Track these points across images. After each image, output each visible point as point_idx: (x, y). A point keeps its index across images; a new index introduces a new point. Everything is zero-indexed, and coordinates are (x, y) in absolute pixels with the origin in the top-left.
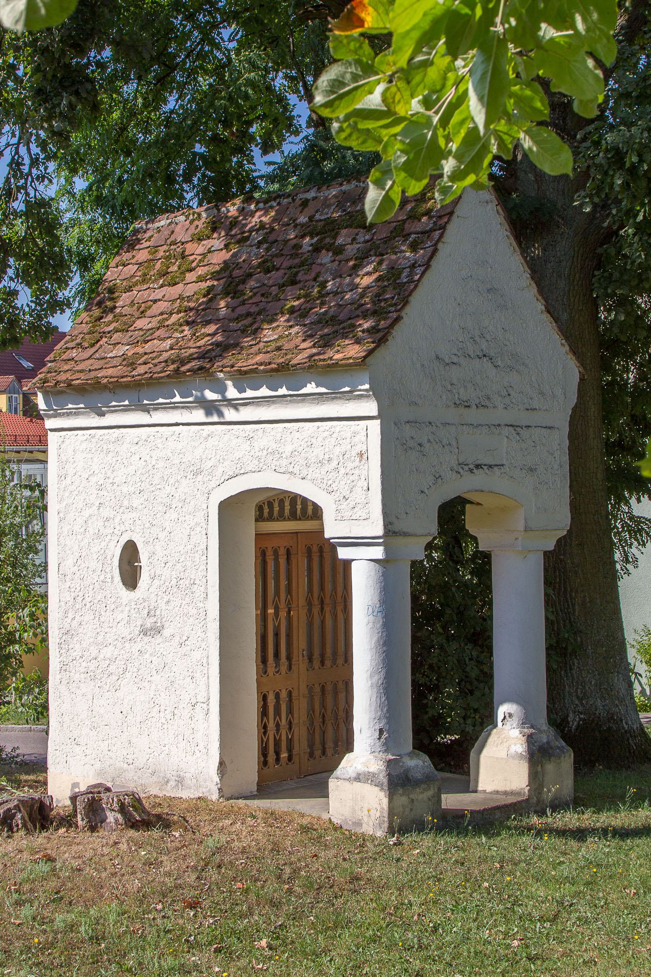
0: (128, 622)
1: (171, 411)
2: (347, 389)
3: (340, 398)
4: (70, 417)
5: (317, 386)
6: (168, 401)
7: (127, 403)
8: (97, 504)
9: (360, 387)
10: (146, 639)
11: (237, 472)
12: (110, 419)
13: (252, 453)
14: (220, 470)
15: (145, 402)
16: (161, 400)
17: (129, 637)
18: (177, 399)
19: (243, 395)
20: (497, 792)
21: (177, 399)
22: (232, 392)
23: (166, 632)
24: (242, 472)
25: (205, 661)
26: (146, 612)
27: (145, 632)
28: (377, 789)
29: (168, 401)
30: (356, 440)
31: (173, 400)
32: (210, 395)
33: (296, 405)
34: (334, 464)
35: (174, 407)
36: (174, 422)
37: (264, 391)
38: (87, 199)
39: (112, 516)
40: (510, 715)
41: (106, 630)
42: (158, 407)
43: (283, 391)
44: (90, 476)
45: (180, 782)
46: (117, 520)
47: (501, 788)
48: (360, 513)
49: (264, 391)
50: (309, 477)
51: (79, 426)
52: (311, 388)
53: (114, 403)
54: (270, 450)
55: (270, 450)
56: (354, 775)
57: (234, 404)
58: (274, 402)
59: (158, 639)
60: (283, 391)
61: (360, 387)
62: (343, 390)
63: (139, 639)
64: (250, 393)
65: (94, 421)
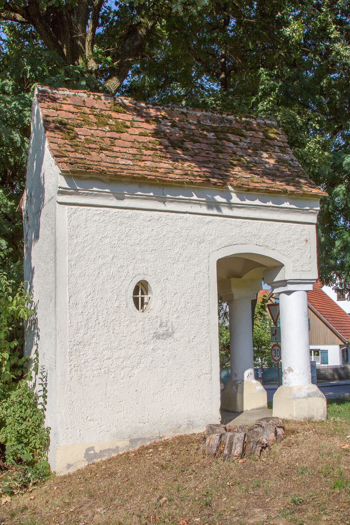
0: (143, 332)
1: (183, 204)
2: (307, 208)
3: (300, 212)
4: (87, 197)
5: (291, 204)
6: (188, 198)
7: (152, 194)
8: (111, 256)
9: (315, 208)
10: (158, 341)
11: (231, 243)
12: (126, 203)
13: (241, 234)
14: (219, 242)
15: (168, 196)
16: (181, 197)
17: (143, 341)
18: (195, 197)
19: (243, 202)
20: (253, 409)
21: (195, 197)
22: (235, 199)
23: (176, 336)
24: (234, 243)
25: (209, 349)
26: (159, 323)
27: (157, 336)
28: (320, 398)
29: (188, 198)
30: (304, 233)
31: (190, 198)
32: (218, 198)
33: (272, 212)
34: (292, 244)
35: (190, 202)
36: (185, 211)
37: (257, 202)
38: (344, 76)
39: (125, 264)
40: (251, 374)
41: (121, 339)
42: (173, 201)
43: (270, 204)
44: (102, 238)
45: (191, 424)
46: (131, 267)
47: (255, 407)
48: (306, 268)
49: (257, 202)
50: (277, 249)
51: (96, 203)
52: (286, 205)
53: (139, 193)
54: (253, 234)
55: (253, 234)
56: (306, 395)
57: (231, 206)
58: (260, 209)
59: (170, 340)
60: (270, 204)
61: (315, 208)
62: (305, 208)
63: (152, 342)
64: (247, 202)
65: (114, 202)
